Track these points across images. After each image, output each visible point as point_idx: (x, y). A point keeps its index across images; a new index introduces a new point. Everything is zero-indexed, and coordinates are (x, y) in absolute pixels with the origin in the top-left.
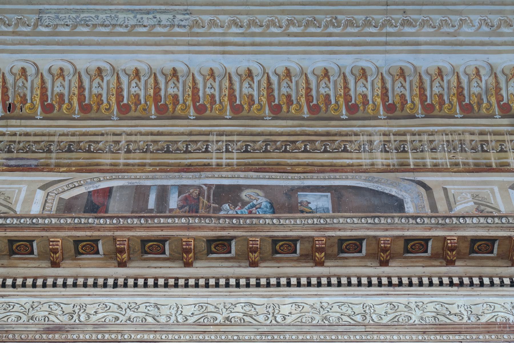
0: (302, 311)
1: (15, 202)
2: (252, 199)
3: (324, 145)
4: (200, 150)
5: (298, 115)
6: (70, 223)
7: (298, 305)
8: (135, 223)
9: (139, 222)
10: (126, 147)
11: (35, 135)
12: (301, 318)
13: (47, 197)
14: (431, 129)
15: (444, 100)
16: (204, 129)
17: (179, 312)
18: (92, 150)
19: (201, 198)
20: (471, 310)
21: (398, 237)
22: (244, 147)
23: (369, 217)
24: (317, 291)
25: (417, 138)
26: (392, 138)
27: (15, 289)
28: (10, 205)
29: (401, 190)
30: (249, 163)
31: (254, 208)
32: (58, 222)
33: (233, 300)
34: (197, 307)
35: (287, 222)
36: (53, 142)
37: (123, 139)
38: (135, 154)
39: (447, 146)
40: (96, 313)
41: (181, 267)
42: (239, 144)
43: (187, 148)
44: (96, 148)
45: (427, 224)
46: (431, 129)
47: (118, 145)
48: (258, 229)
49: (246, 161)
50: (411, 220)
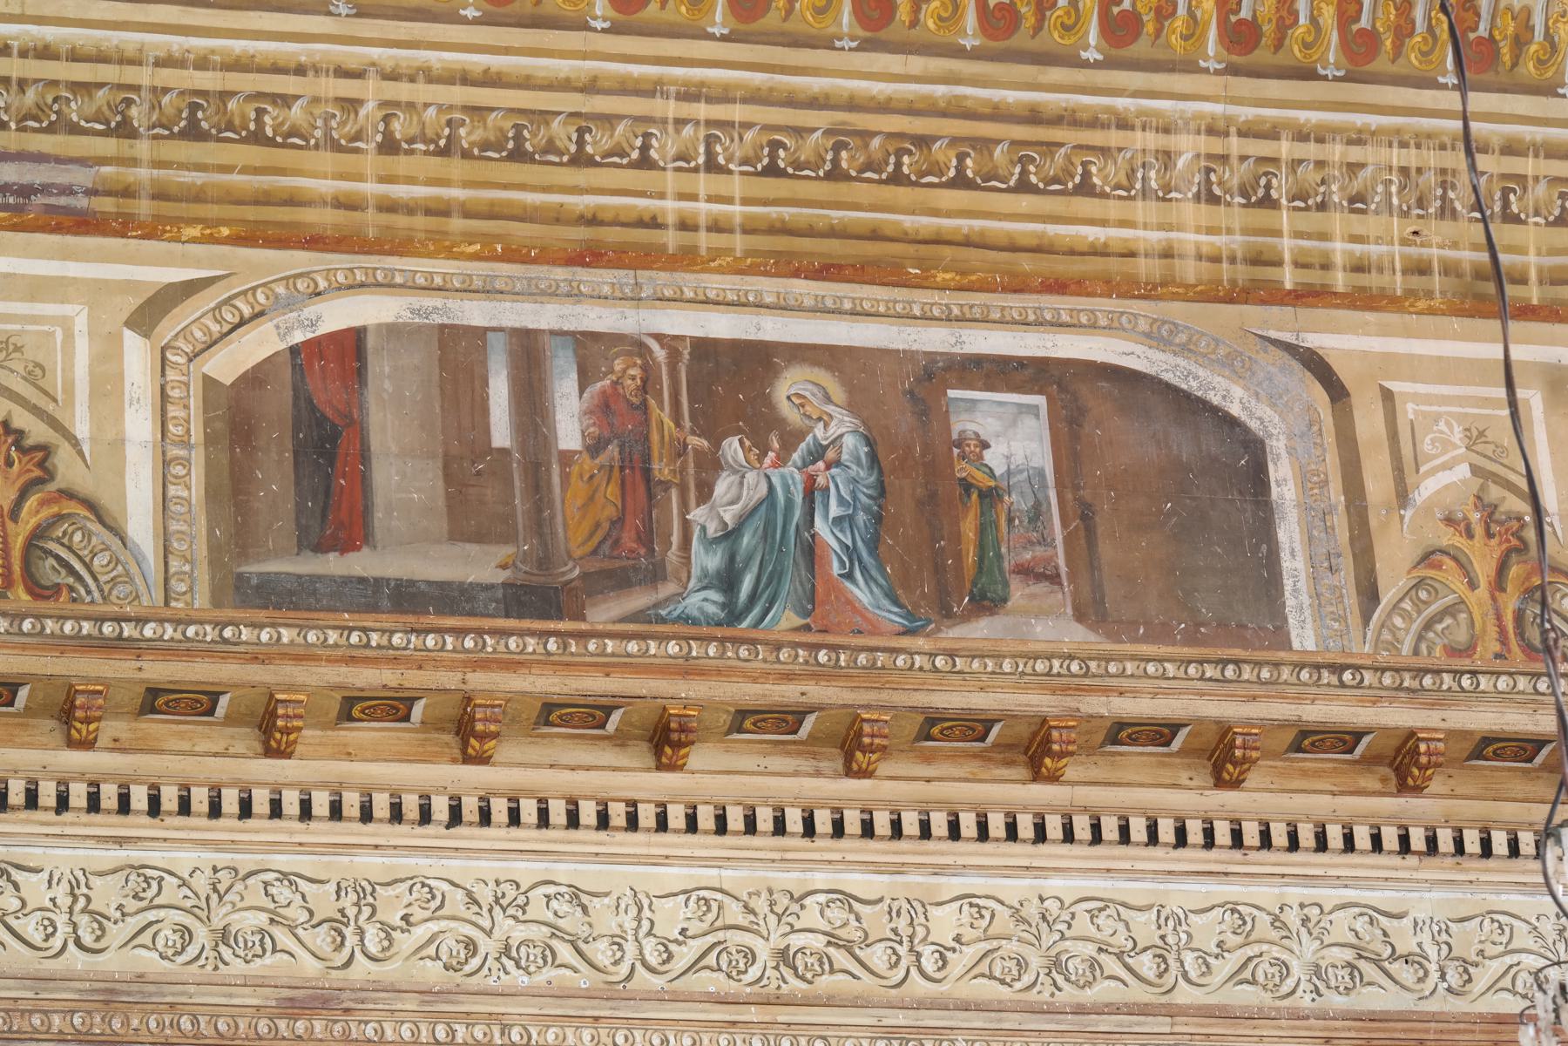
0: (991, 932)
1: (64, 391)
2: (810, 417)
3: (1020, 160)
4: (622, 154)
5: (946, 37)
6: (336, 645)
7: (977, 906)
8: (530, 649)
9: (540, 650)
10: (381, 127)
11: (75, 56)
12: (989, 960)
13: (163, 374)
14: (1359, 119)
15: (1413, 22)
16: (636, 70)
17: (646, 925)
18: (269, 132)
19: (652, 402)
20: (1449, 940)
21: (1284, 725)
22: (766, 151)
23: (1208, 662)
24: (1030, 856)
25: (1311, 150)
26: (1235, 145)
27: (157, 821)
28: (51, 407)
29: (1257, 394)
30: (783, 221)
31: (821, 464)
32: (300, 640)
33: (790, 879)
34: (692, 903)
35: (976, 664)
36: (136, 88)
37: (371, 91)
38: (411, 158)
39: (1402, 188)
40: (408, 923)
41: (648, 770)
42: (749, 136)
43: (581, 143)
44: (282, 124)
45: (1370, 687)
46: (1359, 119)
47: (352, 116)
48: (888, 682)
49: (773, 211)
50: (1325, 673)
